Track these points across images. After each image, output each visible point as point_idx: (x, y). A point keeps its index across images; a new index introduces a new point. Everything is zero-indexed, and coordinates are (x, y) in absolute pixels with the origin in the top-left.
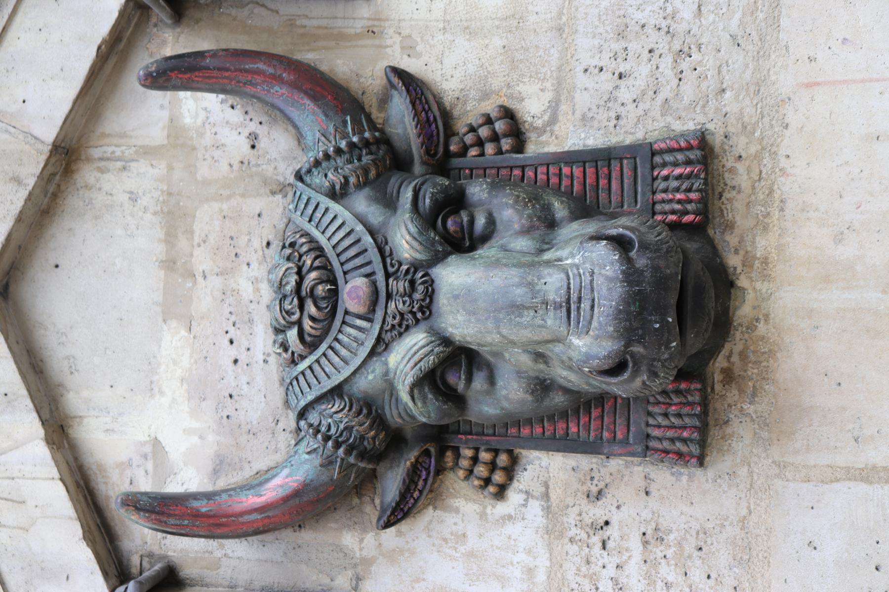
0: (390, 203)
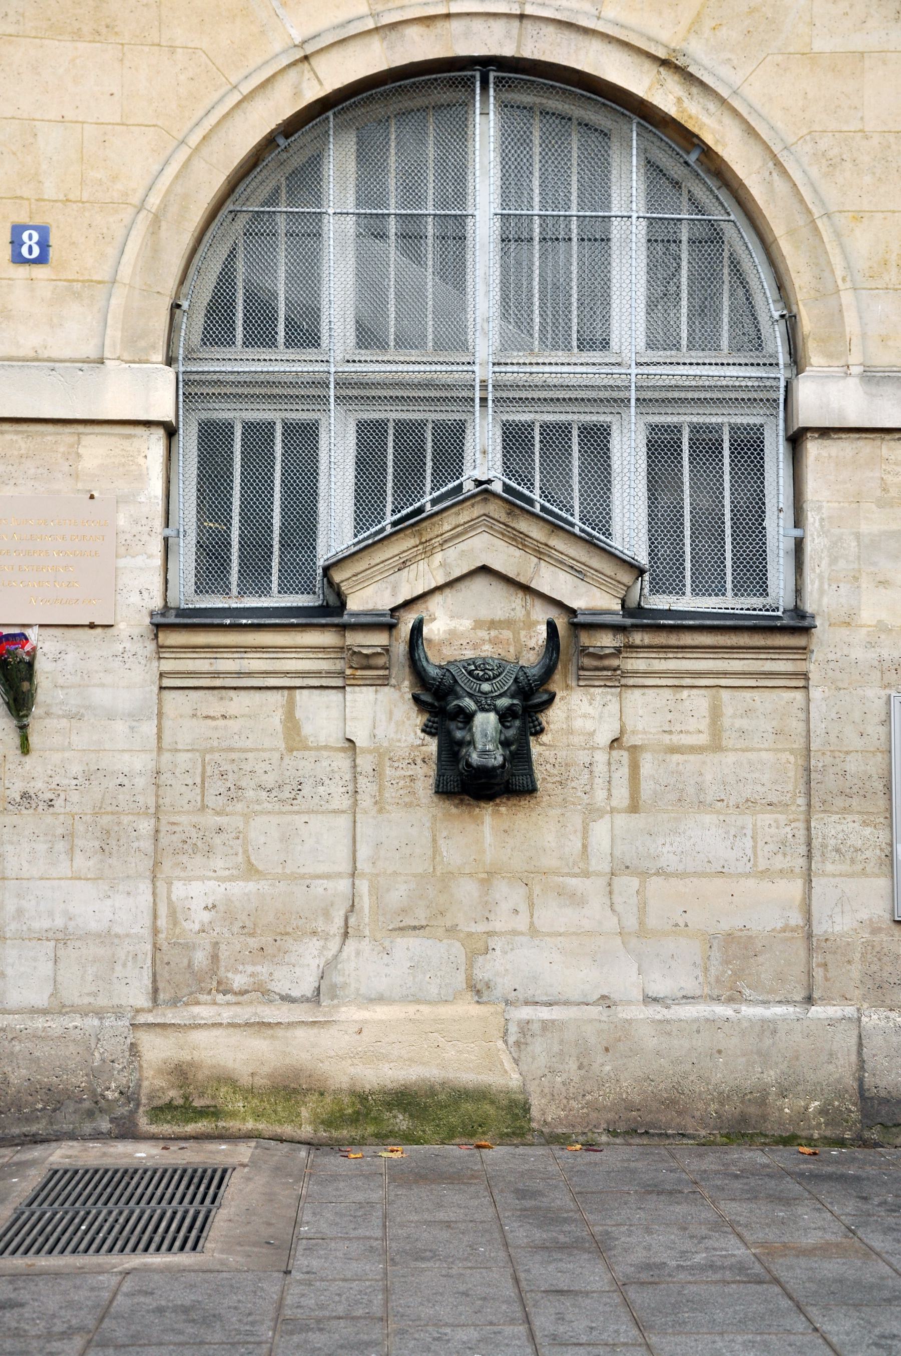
0: (512, 697)
